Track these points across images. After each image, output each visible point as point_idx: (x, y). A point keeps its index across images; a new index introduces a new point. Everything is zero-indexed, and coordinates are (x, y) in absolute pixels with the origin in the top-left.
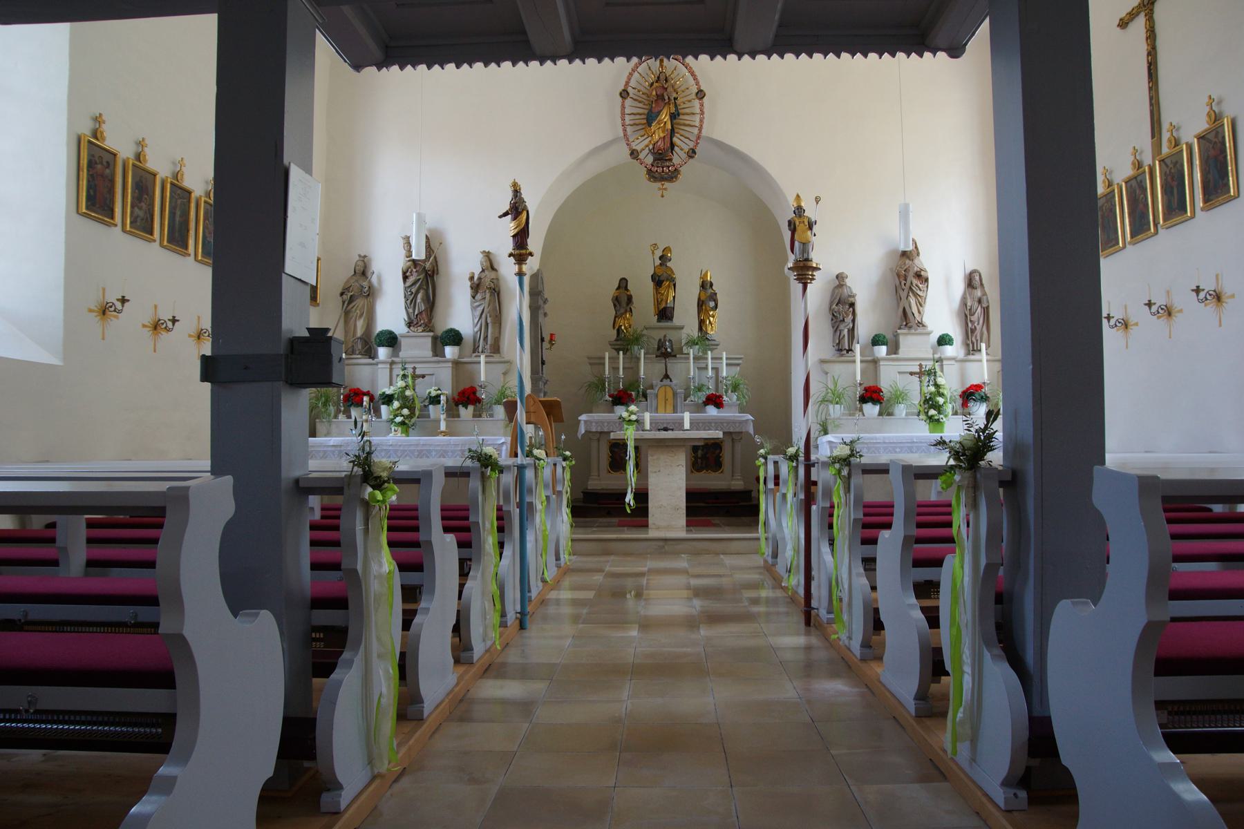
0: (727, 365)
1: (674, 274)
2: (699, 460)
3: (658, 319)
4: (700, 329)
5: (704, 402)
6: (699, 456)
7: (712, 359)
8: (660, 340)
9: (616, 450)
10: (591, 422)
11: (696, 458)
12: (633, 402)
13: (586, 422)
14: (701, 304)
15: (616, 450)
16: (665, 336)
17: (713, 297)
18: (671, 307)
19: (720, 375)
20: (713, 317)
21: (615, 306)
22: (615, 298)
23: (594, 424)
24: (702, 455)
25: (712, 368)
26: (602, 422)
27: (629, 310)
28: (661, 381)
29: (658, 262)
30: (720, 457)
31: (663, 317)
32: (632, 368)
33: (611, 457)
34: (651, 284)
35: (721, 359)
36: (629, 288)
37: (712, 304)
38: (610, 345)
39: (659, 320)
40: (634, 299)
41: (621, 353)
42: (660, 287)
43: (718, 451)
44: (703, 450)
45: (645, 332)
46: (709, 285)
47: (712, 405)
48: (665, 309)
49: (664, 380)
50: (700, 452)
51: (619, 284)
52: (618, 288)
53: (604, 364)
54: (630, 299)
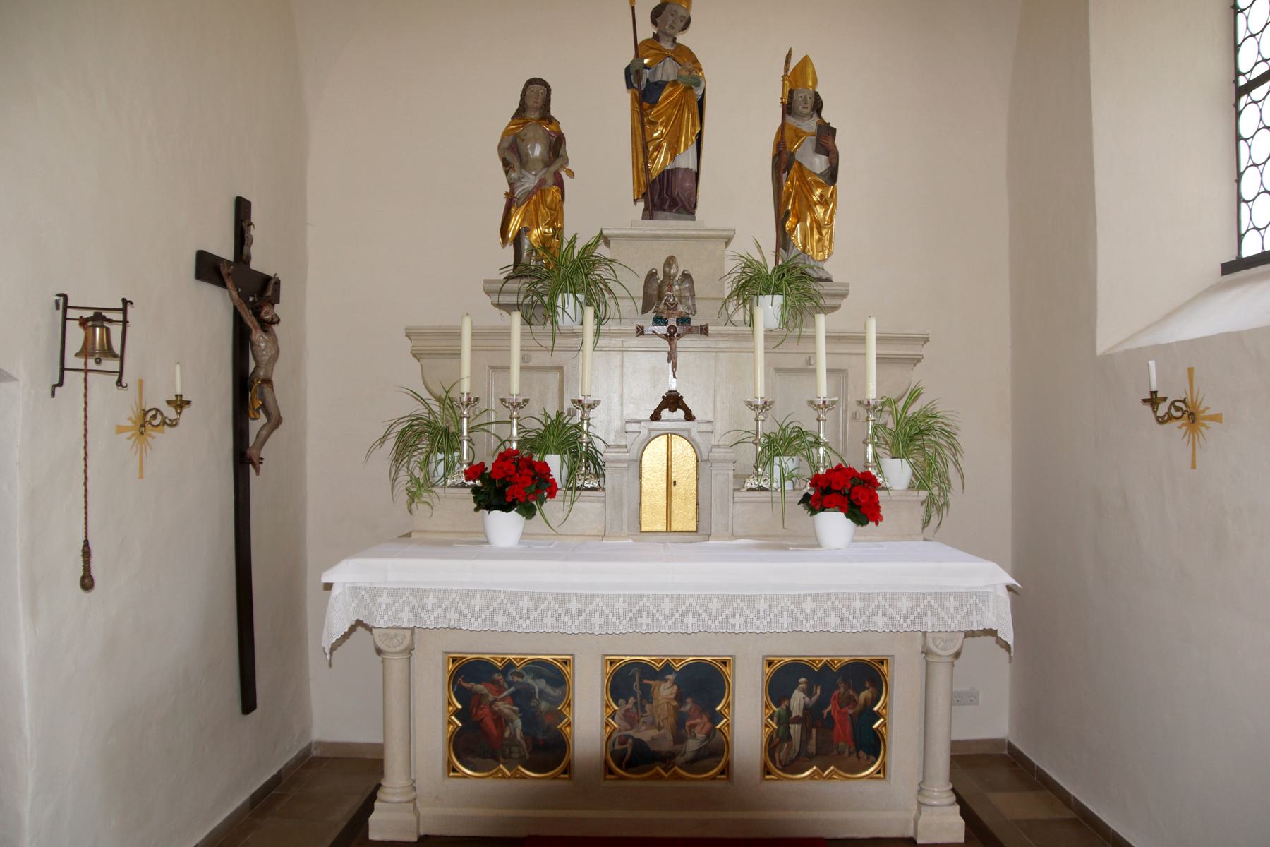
0: (881, 359)
1: (700, 70)
2: (795, 729)
3: (646, 209)
4: (783, 239)
5: (806, 499)
6: (796, 710)
7: (829, 338)
8: (652, 275)
9: (480, 687)
10: (374, 592)
11: (785, 720)
12: (552, 494)
13: (355, 590)
14: (783, 161)
15: (480, 687)
16: (670, 261)
17: (825, 139)
18: (687, 170)
19: (852, 399)
20: (824, 202)
21: (506, 164)
22: (506, 145)
23: (384, 600)
24: (806, 708)
25: (829, 371)
26: (420, 594)
27: (550, 181)
28: (656, 416)
29: (647, 31)
30: (877, 716)
31: (663, 201)
32: (559, 369)
33: (457, 714)
34: (624, 100)
35: (862, 339)
36: (554, 112)
37: (819, 164)
38: (488, 293)
39: (649, 214)
40: (571, 148)
41: (516, 317)
42: (654, 103)
43: (865, 695)
44: (808, 693)
45: (602, 250)
46: (810, 102)
47: (842, 510)
48: (668, 176)
49: (665, 413)
50: (798, 700)
51: (523, 96)
52: (521, 113)
53: (457, 355)
54: (556, 145)
